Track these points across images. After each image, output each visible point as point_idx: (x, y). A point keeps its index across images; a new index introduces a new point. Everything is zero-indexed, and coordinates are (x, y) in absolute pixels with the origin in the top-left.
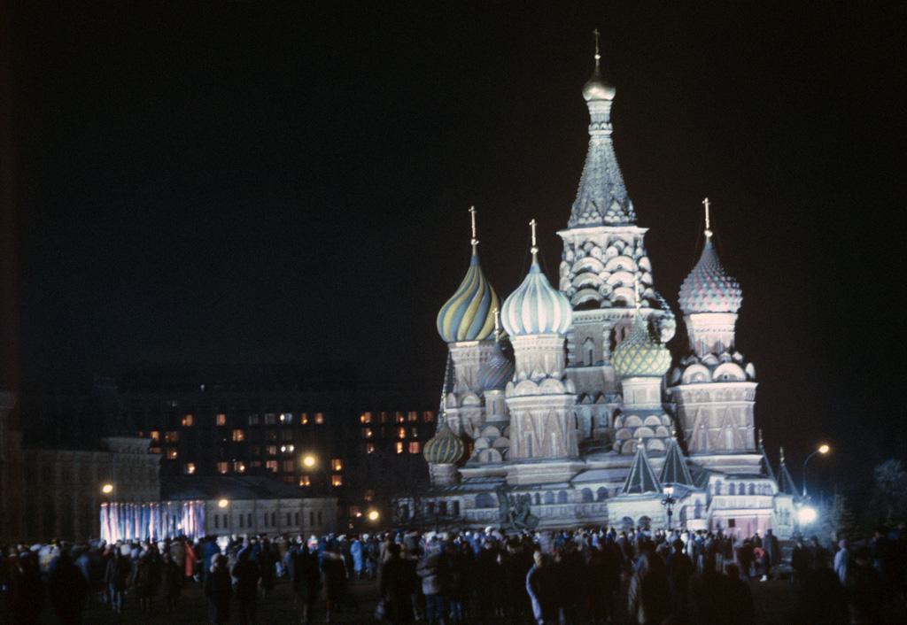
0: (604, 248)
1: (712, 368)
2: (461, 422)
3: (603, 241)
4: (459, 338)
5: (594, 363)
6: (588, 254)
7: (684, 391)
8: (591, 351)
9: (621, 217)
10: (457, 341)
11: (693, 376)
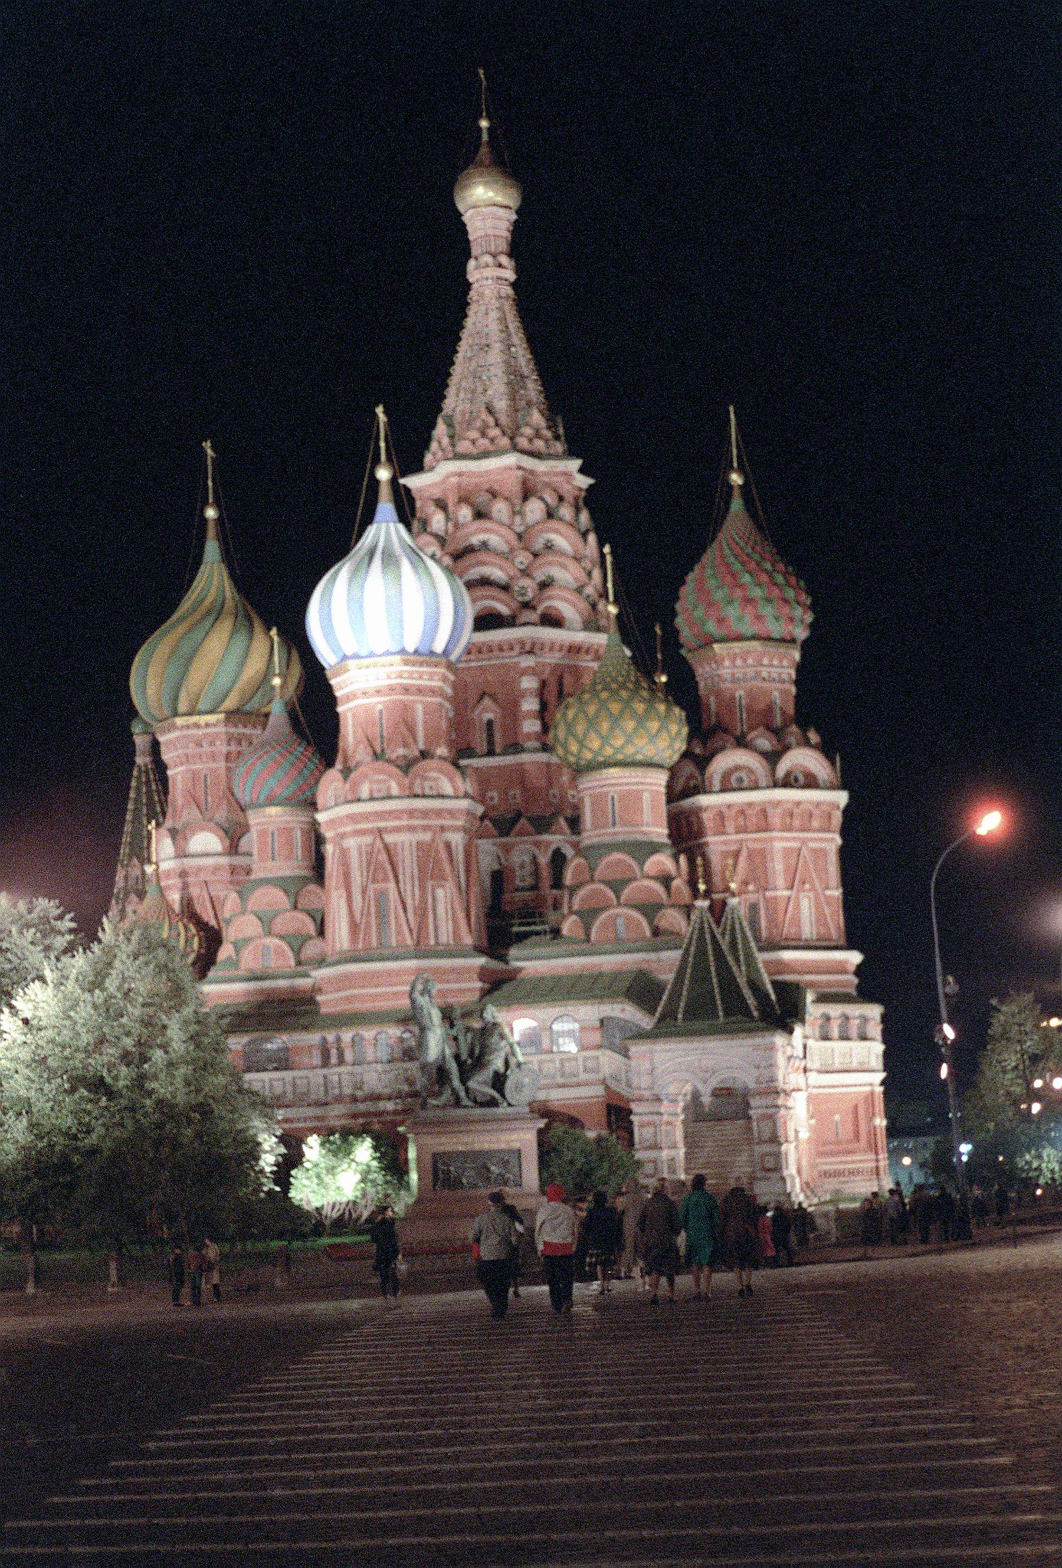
0: (518, 501)
1: (772, 758)
2: (185, 887)
3: (512, 485)
4: (182, 707)
5: (498, 750)
6: (480, 515)
7: (706, 809)
8: (490, 723)
9: (547, 441)
10: (176, 714)
11: (726, 776)
